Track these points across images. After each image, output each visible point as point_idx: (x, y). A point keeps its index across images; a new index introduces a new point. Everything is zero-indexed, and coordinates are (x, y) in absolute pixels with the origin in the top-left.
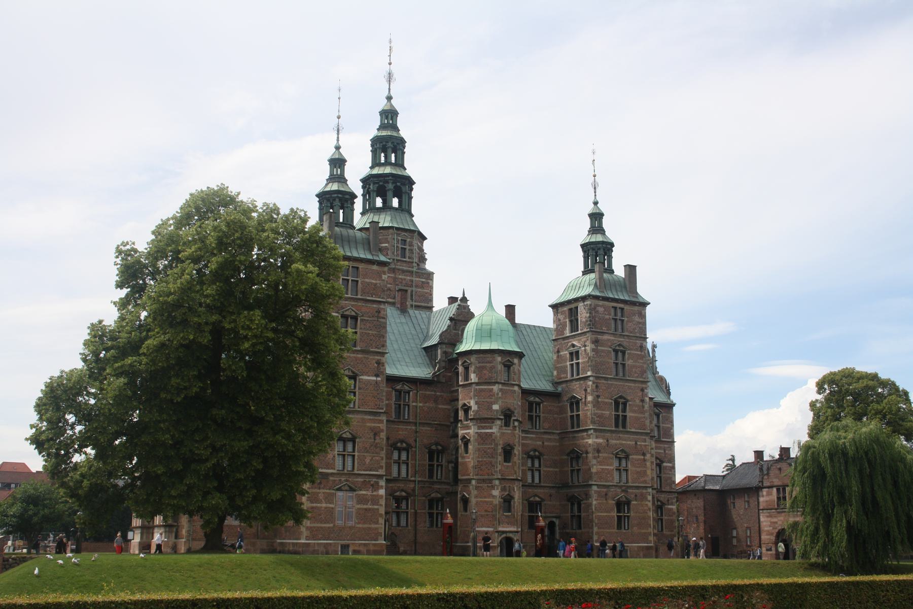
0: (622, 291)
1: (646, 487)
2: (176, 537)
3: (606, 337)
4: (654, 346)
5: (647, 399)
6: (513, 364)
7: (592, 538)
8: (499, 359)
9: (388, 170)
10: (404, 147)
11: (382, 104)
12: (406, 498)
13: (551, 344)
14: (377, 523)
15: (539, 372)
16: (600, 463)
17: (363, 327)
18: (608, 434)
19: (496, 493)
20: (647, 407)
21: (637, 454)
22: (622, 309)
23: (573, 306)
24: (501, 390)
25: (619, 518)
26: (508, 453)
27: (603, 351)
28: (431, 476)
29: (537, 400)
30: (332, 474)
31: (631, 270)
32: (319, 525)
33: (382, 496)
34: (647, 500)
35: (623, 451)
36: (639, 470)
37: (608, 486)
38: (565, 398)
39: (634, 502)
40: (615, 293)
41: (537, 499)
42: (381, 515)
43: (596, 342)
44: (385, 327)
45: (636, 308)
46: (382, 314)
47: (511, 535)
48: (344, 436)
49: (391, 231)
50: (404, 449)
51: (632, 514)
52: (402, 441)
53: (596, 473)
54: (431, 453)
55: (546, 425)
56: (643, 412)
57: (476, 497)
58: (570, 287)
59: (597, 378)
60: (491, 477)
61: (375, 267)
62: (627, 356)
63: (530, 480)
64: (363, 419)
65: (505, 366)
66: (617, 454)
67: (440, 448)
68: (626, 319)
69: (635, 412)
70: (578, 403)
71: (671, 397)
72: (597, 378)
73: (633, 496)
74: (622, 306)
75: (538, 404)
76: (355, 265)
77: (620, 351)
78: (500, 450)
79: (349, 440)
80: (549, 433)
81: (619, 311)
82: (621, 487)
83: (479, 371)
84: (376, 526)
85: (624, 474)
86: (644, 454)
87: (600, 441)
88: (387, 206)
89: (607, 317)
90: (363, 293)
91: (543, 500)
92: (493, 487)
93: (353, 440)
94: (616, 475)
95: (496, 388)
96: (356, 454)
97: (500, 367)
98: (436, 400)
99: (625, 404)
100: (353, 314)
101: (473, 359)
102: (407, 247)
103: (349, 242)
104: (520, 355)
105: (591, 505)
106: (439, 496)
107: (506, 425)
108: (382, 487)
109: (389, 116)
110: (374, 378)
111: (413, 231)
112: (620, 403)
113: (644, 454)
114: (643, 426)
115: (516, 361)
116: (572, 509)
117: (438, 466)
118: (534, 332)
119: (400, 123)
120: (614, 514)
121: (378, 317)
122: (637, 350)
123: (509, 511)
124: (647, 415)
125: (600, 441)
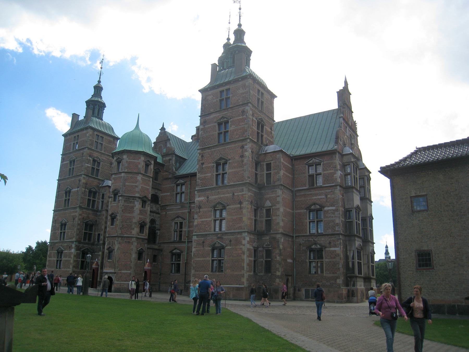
3: (212, 116)
30: (57, 243)
35: (219, 203)
39: (229, 247)
45: (240, 83)
47: (111, 275)
53: (197, 225)
61: (85, 132)
66: (215, 207)
73: (228, 242)
82: (217, 234)
84: (69, 270)
86: (241, 203)
87: (202, 198)
99: (225, 163)
110: (77, 189)
115: (125, 157)
125: (202, 198)
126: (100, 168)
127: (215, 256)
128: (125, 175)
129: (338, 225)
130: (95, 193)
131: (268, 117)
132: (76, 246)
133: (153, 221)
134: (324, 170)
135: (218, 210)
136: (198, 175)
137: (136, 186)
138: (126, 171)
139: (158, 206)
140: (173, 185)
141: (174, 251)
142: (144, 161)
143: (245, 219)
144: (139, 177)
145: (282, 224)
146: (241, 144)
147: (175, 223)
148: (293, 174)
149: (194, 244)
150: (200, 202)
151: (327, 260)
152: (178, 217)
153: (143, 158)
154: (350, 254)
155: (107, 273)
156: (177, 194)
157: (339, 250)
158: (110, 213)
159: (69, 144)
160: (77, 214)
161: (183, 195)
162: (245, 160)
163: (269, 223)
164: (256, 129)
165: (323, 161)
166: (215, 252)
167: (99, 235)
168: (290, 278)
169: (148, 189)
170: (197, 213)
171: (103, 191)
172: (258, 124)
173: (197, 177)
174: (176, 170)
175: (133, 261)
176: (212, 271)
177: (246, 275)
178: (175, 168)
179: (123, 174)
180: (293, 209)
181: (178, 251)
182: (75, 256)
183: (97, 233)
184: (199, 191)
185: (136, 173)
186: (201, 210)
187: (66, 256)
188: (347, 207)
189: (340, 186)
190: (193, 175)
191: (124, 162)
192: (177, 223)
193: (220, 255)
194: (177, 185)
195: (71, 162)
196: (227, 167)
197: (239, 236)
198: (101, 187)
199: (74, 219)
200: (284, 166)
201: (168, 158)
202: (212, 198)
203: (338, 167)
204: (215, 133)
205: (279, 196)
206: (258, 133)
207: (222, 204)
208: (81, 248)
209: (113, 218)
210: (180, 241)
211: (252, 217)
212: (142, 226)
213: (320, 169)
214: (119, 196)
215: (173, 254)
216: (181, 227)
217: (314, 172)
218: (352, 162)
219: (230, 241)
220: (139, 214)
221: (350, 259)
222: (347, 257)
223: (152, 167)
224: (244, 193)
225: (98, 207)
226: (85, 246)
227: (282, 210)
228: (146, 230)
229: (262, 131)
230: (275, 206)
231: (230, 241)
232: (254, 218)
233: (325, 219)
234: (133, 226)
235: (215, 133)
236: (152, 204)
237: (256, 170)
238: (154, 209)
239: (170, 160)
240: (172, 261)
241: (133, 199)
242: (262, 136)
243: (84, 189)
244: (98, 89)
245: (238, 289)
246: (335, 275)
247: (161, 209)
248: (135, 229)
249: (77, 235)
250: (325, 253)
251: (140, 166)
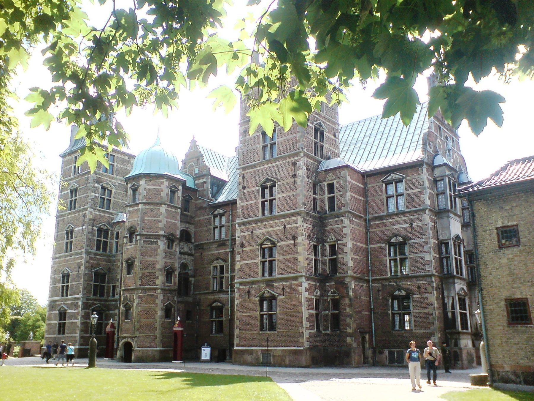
1: (296, 278)
21: (287, 239)
35: (267, 239)
37: (253, 283)
39: (282, 297)
47: (129, 340)
53: (239, 270)
66: (261, 244)
73: (280, 290)
86: (294, 238)
110: (81, 228)
115: (142, 182)
126: (112, 199)
127: (265, 310)
128: (144, 207)
129: (428, 262)
130: (106, 231)
131: (329, 121)
132: (83, 303)
133: (184, 266)
134: (407, 189)
135: (267, 248)
136: (238, 202)
137: (160, 221)
138: (144, 201)
139: (191, 245)
140: (209, 216)
141: (214, 305)
142: (167, 187)
143: (300, 259)
144: (163, 209)
145: (351, 264)
146: (292, 159)
147: (214, 267)
148: (366, 196)
149: (237, 295)
151: (416, 311)
152: (217, 259)
153: (166, 183)
154: (448, 302)
155: (124, 338)
156: (214, 228)
157: (433, 298)
158: (125, 257)
159: (68, 167)
160: (83, 261)
161: (223, 229)
162: (299, 180)
163: (334, 263)
164: (313, 138)
165: (406, 177)
166: (265, 303)
167: (114, 287)
168: (367, 337)
169: (175, 224)
171: (117, 229)
172: (316, 130)
173: (238, 206)
174: (213, 197)
175: (158, 320)
176: (262, 329)
177: (306, 334)
178: (212, 194)
179: (140, 206)
180: (367, 244)
181: (219, 304)
182: (82, 316)
183: (111, 285)
185: (158, 204)
186: (244, 249)
188: (441, 238)
189: (430, 210)
190: (232, 203)
191: (141, 190)
192: (217, 267)
193: (270, 308)
194: (215, 216)
195: (72, 192)
196: (275, 189)
197: (294, 282)
198: (114, 223)
199: (79, 268)
200: (352, 185)
201: (201, 181)
202: (257, 232)
203: (427, 184)
204: (258, 146)
205: (345, 227)
206: (316, 144)
207: (270, 240)
208: (90, 306)
209: (130, 265)
210: (221, 291)
211: (310, 256)
212: (169, 273)
213: (401, 188)
214: (136, 235)
215: (213, 308)
216: (222, 272)
217: (394, 193)
218: (448, 176)
219: (283, 289)
220: (165, 258)
221: (449, 309)
222: (444, 306)
223: (180, 194)
224: (298, 225)
225: (111, 250)
226: (95, 302)
227: (350, 245)
228: (176, 279)
229: (322, 140)
230: (341, 240)
231: (283, 289)
232: (313, 257)
233: (411, 256)
234: (157, 274)
235: (258, 146)
236: (181, 243)
237: (315, 193)
238: (186, 249)
239: (204, 182)
240: (212, 317)
241: (155, 239)
242: (322, 147)
243: (91, 227)
245: (295, 352)
246: (428, 331)
247: (195, 249)
248: (160, 278)
249: (84, 288)
250: (413, 301)
251: (163, 194)
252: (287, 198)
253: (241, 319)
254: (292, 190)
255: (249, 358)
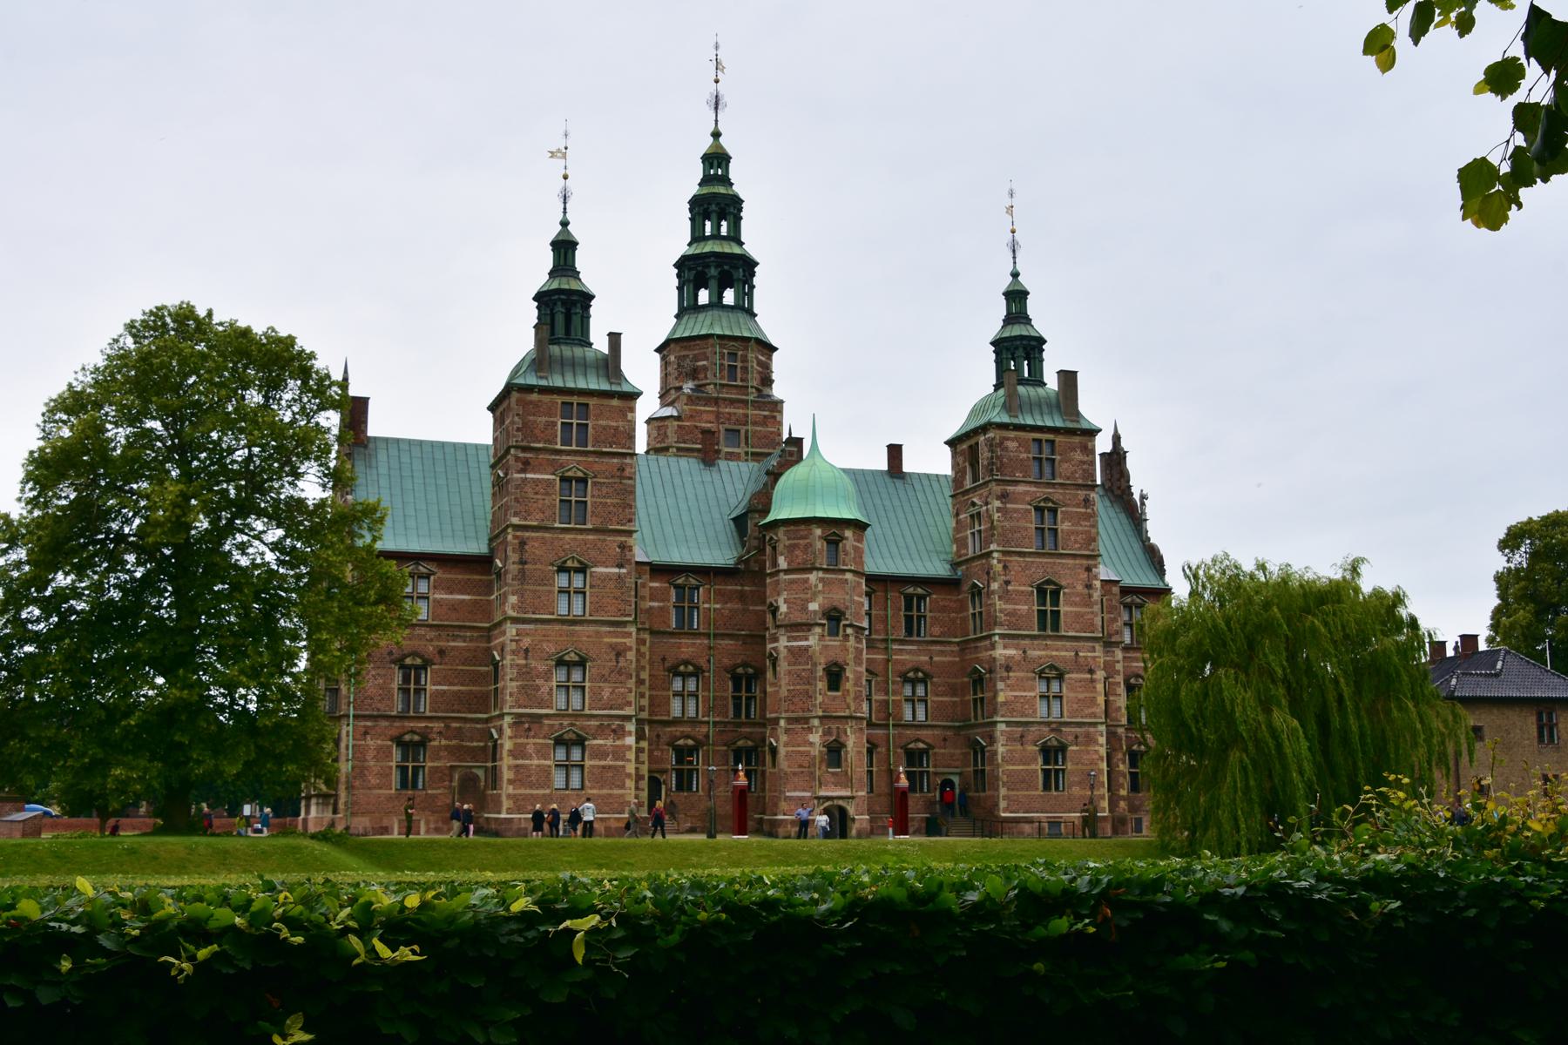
0: (1051, 413)
1: (1095, 725)
2: (335, 811)
3: (1021, 488)
4: (1143, 497)
5: (1097, 584)
6: (843, 538)
7: (997, 805)
8: (818, 532)
9: (708, 247)
10: (741, 210)
11: (706, 143)
12: (692, 750)
13: (950, 501)
14: (623, 786)
15: (930, 547)
16: (1012, 688)
17: (596, 493)
18: (1027, 642)
19: (815, 738)
20: (1096, 595)
21: (1079, 671)
22: (1052, 442)
23: (972, 442)
24: (821, 580)
25: (1046, 773)
26: (835, 677)
27: (1016, 511)
28: (737, 713)
29: (920, 591)
30: (547, 716)
31: (1068, 379)
32: (528, 791)
33: (630, 748)
34: (1096, 742)
35: (1052, 667)
36: (1081, 696)
38: (966, 587)
40: (1038, 417)
41: (921, 745)
42: (629, 775)
43: (1004, 497)
44: (633, 492)
45: (1077, 439)
46: (627, 473)
47: (841, 803)
48: (567, 658)
49: (711, 341)
50: (691, 675)
51: (1069, 766)
52: (686, 663)
53: (1005, 703)
54: (736, 680)
55: (936, 630)
56: (1089, 604)
57: (786, 745)
58: (974, 412)
59: (1005, 553)
60: (807, 715)
61: (615, 402)
62: (1059, 516)
63: (908, 716)
64: (598, 632)
65: (829, 542)
66: (1042, 671)
67: (751, 671)
68: (1058, 458)
69: (1075, 604)
70: (980, 593)
71: (1167, 578)
72: (1005, 553)
73: (1071, 738)
74: (1051, 437)
75: (921, 598)
76: (583, 400)
77: (1046, 510)
78: (820, 673)
79: (575, 664)
80: (941, 643)
81: (1045, 446)
82: (1048, 724)
83: (791, 549)
85: (1056, 706)
86: (1091, 671)
87: (1011, 652)
88: (716, 303)
89: (1024, 456)
90: (596, 442)
91: (931, 747)
92: (810, 730)
93: (582, 663)
94: (1041, 709)
95: (813, 577)
96: (587, 684)
97: (819, 545)
98: (742, 597)
99: (1056, 595)
100: (580, 474)
101: (781, 531)
102: (739, 364)
103: (562, 365)
104: (859, 526)
105: (995, 753)
106: (750, 743)
107: (830, 634)
108: (630, 733)
109: (716, 160)
110: (616, 570)
111: (747, 339)
112: (1048, 592)
113: (1091, 671)
114: (1091, 627)
115: (848, 533)
116: (976, 760)
117: (748, 699)
118: (935, 485)
119: (734, 173)
120: (1038, 766)
121: (622, 478)
122: (1078, 506)
123: (839, 766)
124: (1097, 608)
125: (1011, 652)
150: (1009, 658)
160: (631, 642)
170: (1003, 679)
184: (1002, 636)
187: (600, 753)
199: (618, 655)
207: (1056, 669)
244: (564, 248)
252: (1078, 615)
253: (1010, 774)
254: (1087, 606)
255: (1027, 828)
